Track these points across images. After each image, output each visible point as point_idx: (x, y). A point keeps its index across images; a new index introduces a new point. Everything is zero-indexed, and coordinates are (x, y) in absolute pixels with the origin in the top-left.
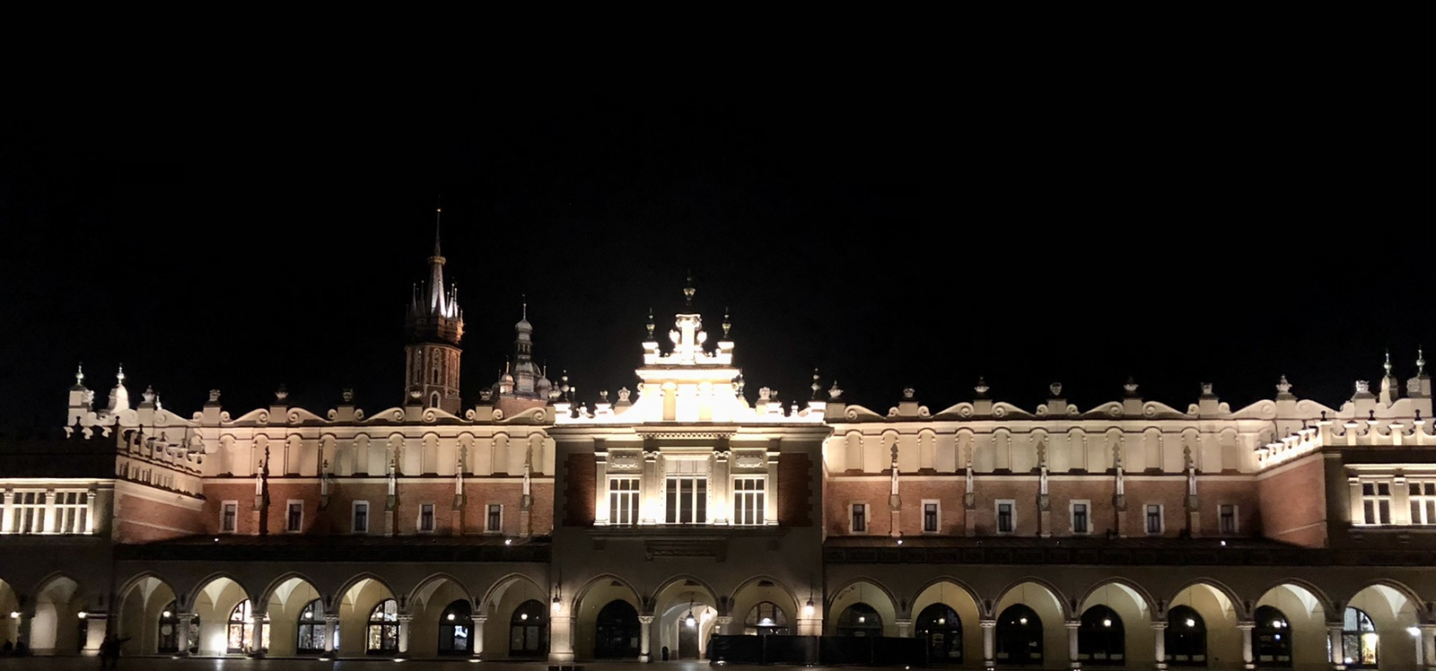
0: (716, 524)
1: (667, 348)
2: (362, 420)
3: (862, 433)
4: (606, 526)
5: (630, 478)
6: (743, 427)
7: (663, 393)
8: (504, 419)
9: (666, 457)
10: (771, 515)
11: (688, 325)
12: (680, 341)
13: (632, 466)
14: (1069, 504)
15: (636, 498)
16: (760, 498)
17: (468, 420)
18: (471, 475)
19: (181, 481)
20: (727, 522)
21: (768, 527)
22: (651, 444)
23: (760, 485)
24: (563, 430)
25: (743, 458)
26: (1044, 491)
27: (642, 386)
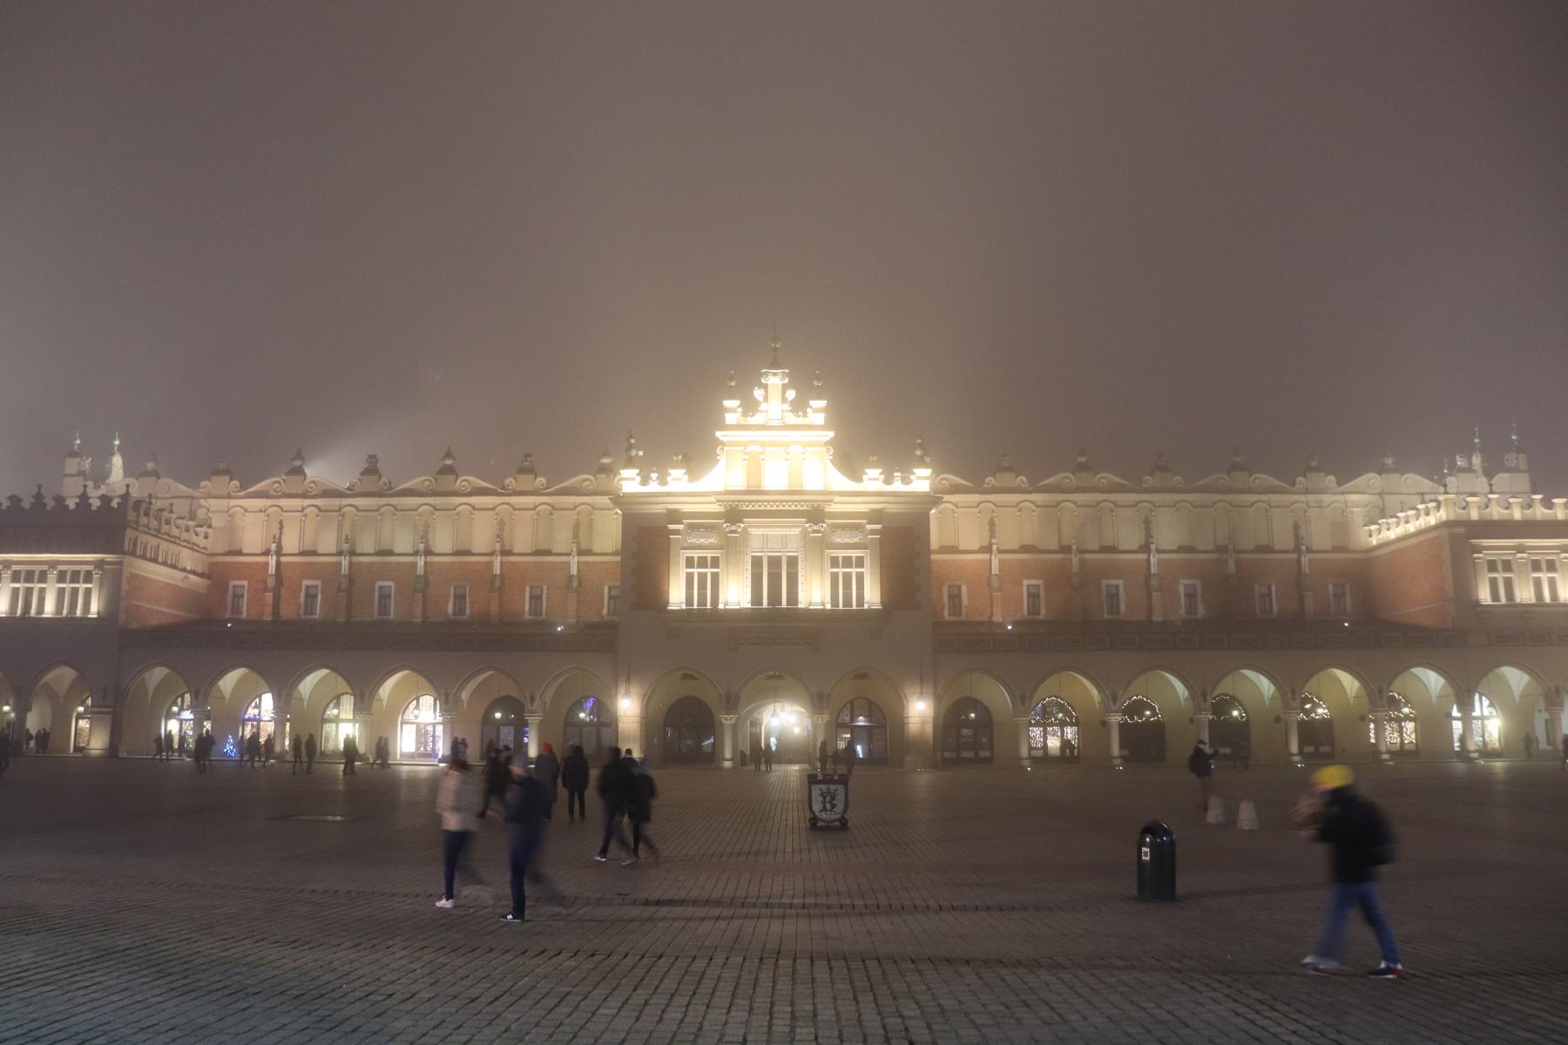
0: (811, 607)
1: (750, 406)
3: (956, 506)
4: (682, 610)
5: (709, 554)
6: (840, 496)
7: (746, 457)
8: (547, 488)
9: (753, 531)
10: (872, 596)
12: (766, 398)
13: (710, 540)
15: (715, 577)
16: (860, 577)
17: (508, 490)
18: (589, 553)
19: (188, 559)
20: (823, 605)
21: (871, 611)
22: (734, 515)
23: (860, 562)
24: (655, 499)
26: (1153, 570)
27: (722, 449)
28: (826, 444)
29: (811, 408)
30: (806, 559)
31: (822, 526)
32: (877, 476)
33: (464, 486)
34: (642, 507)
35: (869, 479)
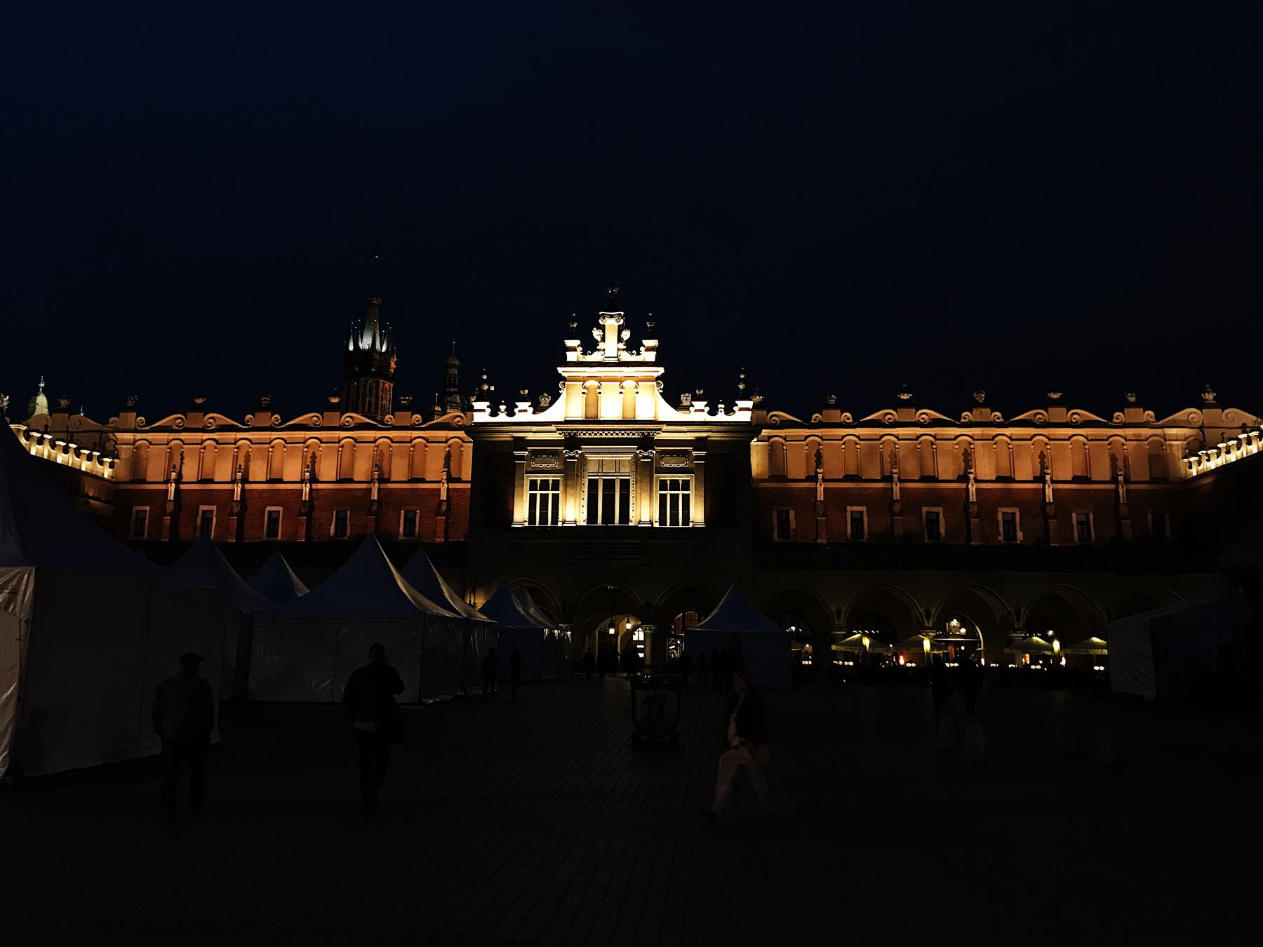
0: (640, 525)
1: (590, 345)
2: (280, 424)
4: (525, 528)
6: (667, 425)
7: (585, 391)
9: (590, 457)
11: (611, 323)
12: (603, 339)
14: (997, 512)
15: (556, 498)
16: (686, 499)
17: (383, 423)
20: (652, 523)
22: (573, 442)
25: (667, 458)
27: (564, 384)
28: (658, 378)
29: (644, 346)
30: (636, 482)
31: (651, 453)
32: (703, 408)
33: (348, 422)
34: (487, 435)
35: (696, 410)
